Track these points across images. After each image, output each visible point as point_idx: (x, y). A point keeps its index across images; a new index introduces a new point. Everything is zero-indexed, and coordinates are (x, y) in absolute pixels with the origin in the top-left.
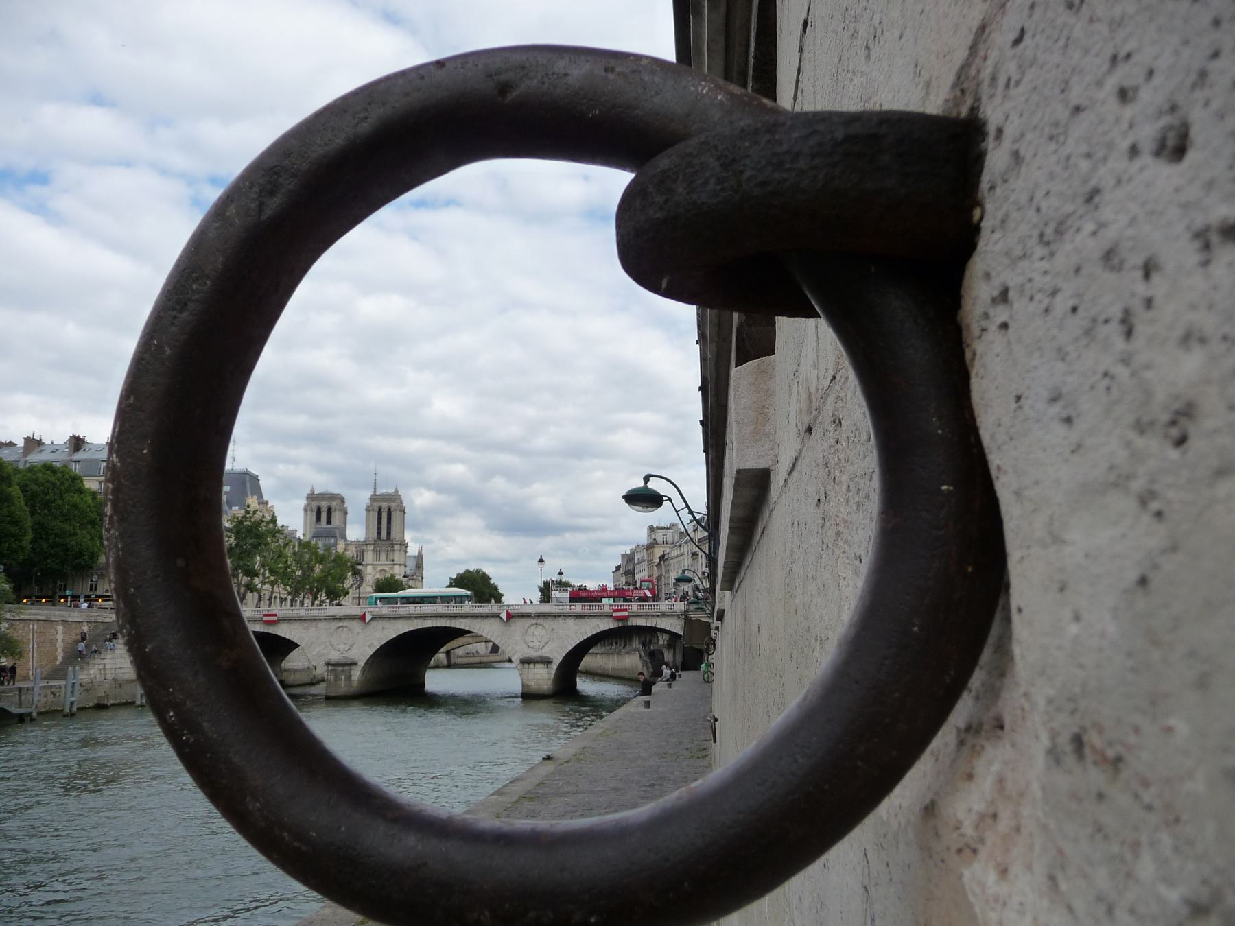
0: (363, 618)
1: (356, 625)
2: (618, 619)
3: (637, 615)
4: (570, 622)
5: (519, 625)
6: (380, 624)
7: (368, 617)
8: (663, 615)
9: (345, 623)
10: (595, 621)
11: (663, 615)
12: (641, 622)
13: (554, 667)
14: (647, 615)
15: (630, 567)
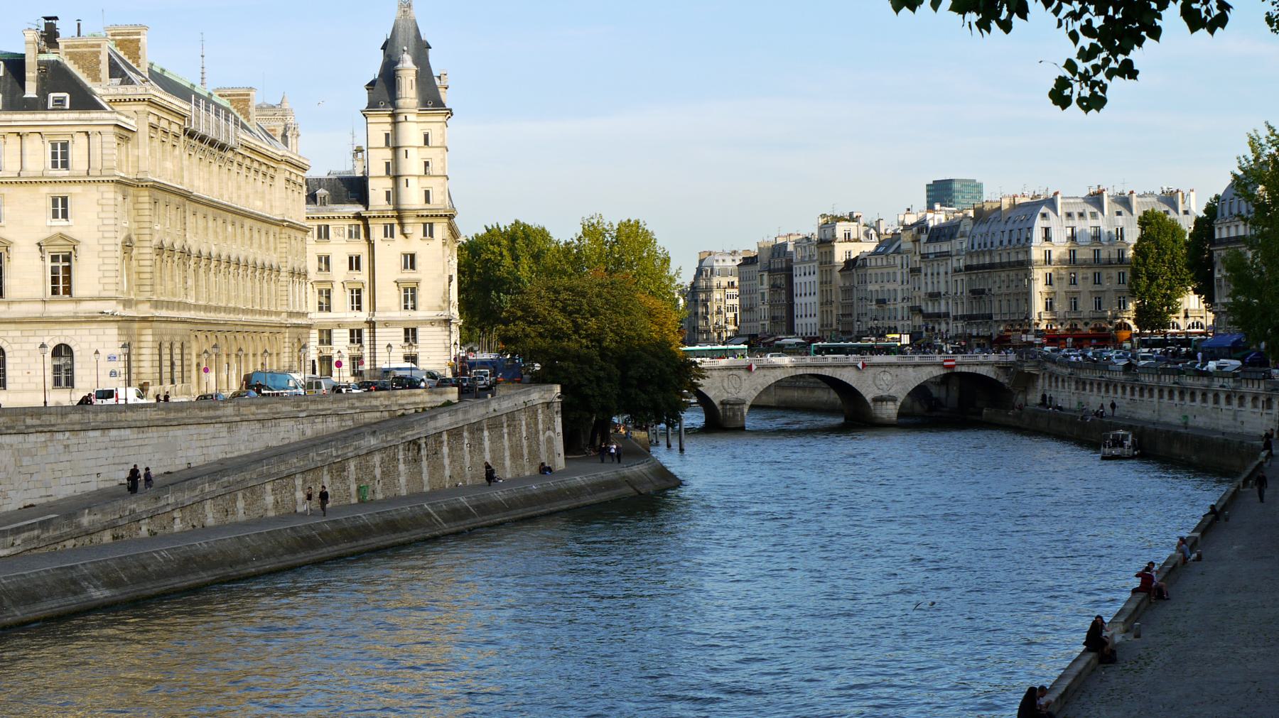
0: (749, 368)
1: (742, 373)
3: (962, 364)
4: (910, 370)
5: (871, 371)
6: (762, 372)
7: (754, 367)
8: (982, 364)
9: (735, 372)
10: (929, 369)
11: (982, 364)
12: (964, 369)
13: (899, 404)
14: (969, 364)
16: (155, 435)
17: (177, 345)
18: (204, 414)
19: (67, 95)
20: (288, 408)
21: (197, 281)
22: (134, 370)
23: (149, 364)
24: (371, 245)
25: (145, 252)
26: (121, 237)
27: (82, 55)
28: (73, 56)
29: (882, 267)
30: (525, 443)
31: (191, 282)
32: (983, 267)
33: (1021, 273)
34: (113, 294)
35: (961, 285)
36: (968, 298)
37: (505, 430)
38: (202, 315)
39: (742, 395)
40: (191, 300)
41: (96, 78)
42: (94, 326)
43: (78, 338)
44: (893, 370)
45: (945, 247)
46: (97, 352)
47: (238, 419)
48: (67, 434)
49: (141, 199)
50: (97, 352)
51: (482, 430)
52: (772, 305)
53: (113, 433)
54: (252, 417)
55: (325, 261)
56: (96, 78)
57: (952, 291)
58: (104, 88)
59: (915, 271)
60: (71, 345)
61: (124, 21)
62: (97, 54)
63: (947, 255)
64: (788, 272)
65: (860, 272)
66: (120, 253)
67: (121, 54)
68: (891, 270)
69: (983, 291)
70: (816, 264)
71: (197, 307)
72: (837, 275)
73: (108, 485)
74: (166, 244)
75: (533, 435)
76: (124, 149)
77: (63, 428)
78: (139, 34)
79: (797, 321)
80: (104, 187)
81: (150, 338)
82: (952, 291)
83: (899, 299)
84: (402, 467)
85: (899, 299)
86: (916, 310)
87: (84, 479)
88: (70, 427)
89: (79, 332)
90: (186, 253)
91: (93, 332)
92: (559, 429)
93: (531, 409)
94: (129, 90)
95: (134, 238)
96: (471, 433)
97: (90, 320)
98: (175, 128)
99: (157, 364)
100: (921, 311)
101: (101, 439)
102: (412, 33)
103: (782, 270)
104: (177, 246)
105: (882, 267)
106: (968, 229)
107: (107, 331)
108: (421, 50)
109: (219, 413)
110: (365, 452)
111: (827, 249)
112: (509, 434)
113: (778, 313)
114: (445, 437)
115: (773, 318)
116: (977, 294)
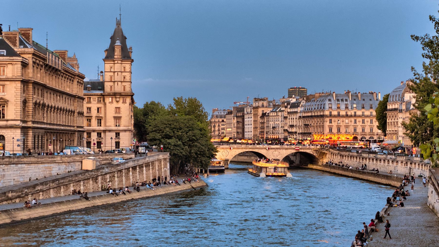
0: (231, 149)
1: (229, 150)
2: (296, 150)
4: (284, 150)
5: (271, 151)
6: (234, 150)
7: (232, 148)
10: (290, 150)
12: (302, 151)
14: (304, 149)
15: (240, 114)
16: (34, 166)
17: (40, 136)
18: (50, 159)
19: (5, 51)
20: (78, 158)
21: (47, 115)
22: (26, 144)
23: (31, 142)
24: (105, 104)
25: (30, 105)
26: (23, 99)
27: (10, 38)
28: (7, 38)
29: (275, 116)
30: (157, 172)
31: (45, 115)
32: (308, 117)
33: (322, 119)
34: (19, 118)
35: (301, 123)
36: (303, 127)
37: (151, 167)
38: (48, 126)
39: (227, 158)
40: (45, 121)
41: (15, 45)
42: (13, 129)
43: (7, 133)
44: (279, 150)
45: (295, 110)
46: (13, 138)
47: (61, 161)
48: (4, 165)
49: (29, 87)
50: (13, 138)
51: (143, 167)
52: (237, 128)
53: (19, 165)
54: (66, 161)
55: (89, 109)
56: (15, 45)
57: (298, 125)
58: (18, 49)
59: (285, 118)
60: (4, 135)
61: (25, 25)
62: (15, 37)
63: (296, 112)
64: (243, 117)
65: (267, 117)
66: (22, 105)
67: (24, 37)
68: (278, 117)
69: (308, 125)
70: (253, 114)
71: (47, 124)
72: (259, 118)
73: (17, 183)
74: (38, 101)
75: (160, 169)
76: (24, 69)
77: (2, 163)
78: (29, 31)
79: (245, 133)
80: (17, 82)
81: (31, 134)
82: (298, 125)
83: (280, 127)
84: (116, 179)
85: (280, 127)
86: (285, 131)
87: (9, 181)
88: (5, 163)
89: (7, 131)
90: (44, 105)
91: (12, 131)
92: (168, 167)
93: (160, 161)
94: (26, 50)
95: (27, 100)
96: (140, 168)
97: (11, 127)
98: (41, 63)
99: (33, 142)
100: (288, 131)
101: (15, 167)
102: (120, 34)
103: (241, 116)
104: (42, 102)
105: (275, 116)
106: (304, 104)
107: (17, 131)
108: (124, 39)
109: (55, 159)
110: (104, 174)
111: (256, 110)
112: (152, 169)
113: (239, 131)
114: (131, 169)
115: (238, 132)
116: (306, 126)
